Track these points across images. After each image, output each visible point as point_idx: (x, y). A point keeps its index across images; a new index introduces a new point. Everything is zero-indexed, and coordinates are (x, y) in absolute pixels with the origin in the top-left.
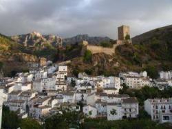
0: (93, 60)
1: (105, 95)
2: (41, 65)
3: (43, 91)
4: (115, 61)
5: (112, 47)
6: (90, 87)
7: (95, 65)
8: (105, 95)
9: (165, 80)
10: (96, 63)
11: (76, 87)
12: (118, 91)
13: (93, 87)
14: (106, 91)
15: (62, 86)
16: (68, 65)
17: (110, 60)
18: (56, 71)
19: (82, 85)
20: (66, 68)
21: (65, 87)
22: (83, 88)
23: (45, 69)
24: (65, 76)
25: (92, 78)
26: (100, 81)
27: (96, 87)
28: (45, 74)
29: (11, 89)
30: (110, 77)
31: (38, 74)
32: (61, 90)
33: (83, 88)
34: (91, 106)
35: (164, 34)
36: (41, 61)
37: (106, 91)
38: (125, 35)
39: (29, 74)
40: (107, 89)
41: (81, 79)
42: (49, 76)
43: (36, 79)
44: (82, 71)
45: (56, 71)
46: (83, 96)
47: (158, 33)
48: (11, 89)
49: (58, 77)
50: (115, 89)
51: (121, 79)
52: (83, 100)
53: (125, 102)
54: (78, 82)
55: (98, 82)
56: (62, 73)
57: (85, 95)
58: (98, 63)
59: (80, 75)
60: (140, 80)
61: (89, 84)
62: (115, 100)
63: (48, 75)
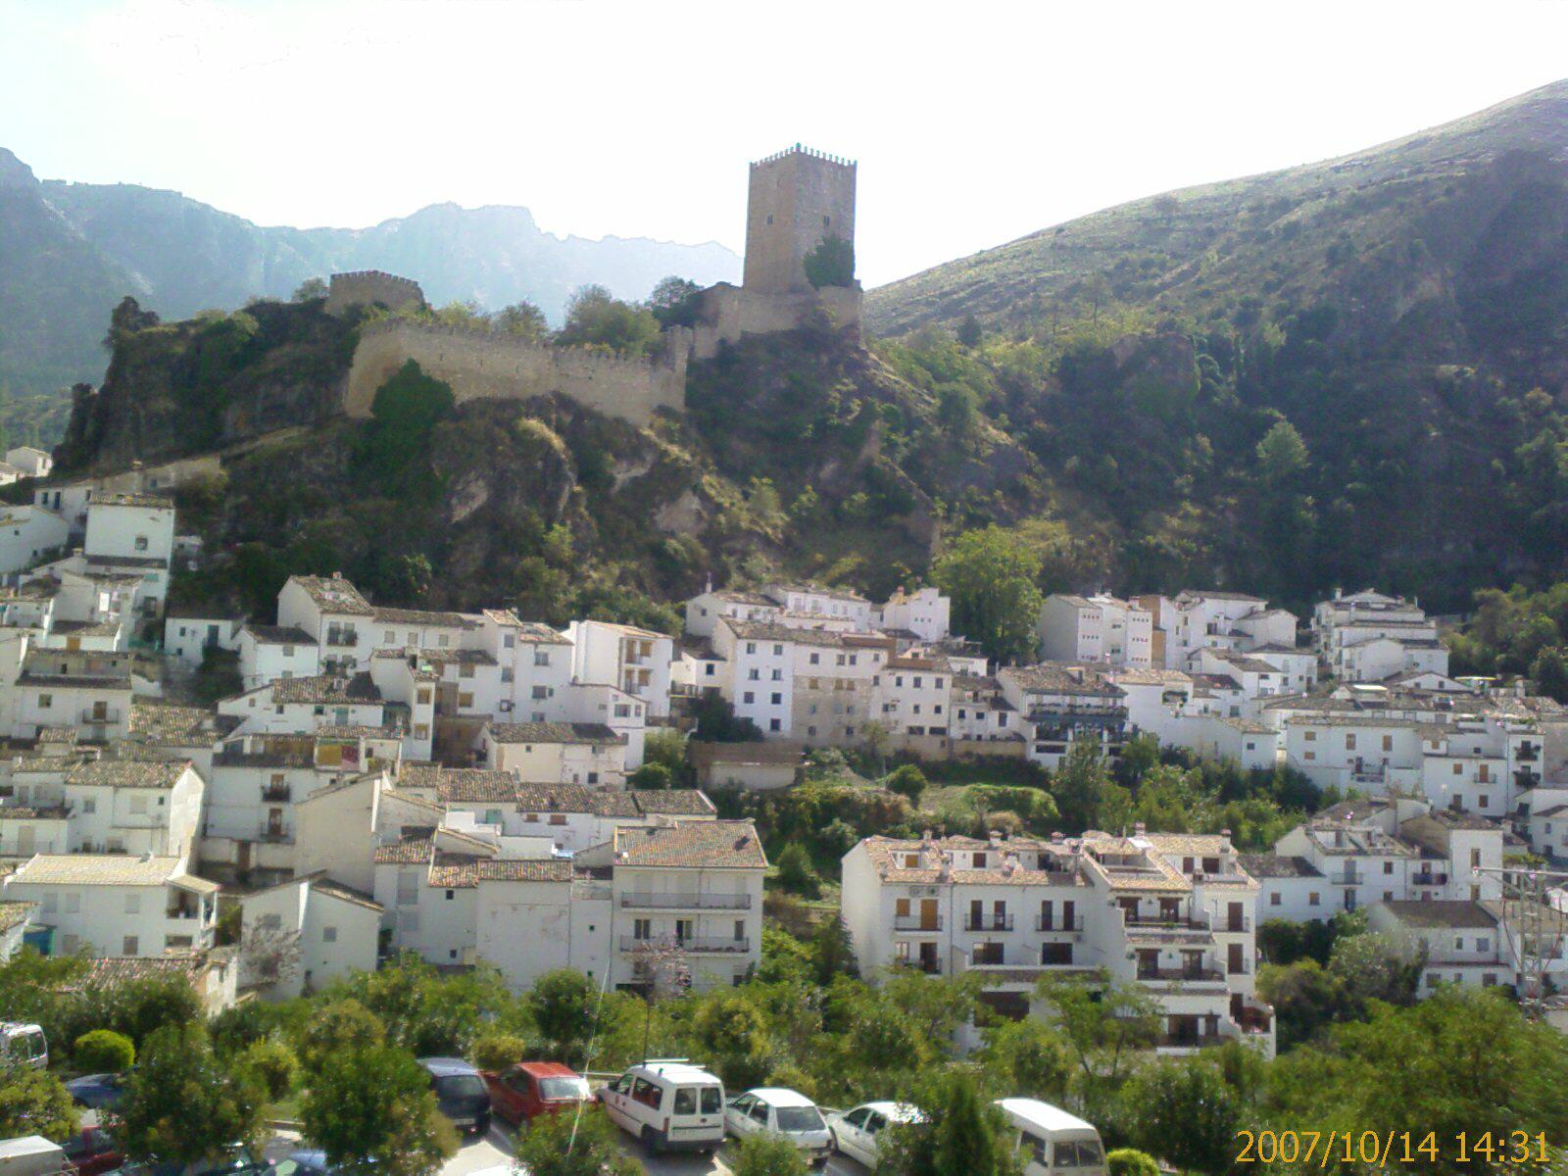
6: (369, 715)
7: (461, 513)
10: (480, 494)
11: (227, 707)
16: (190, 505)
17: (623, 474)
18: (52, 555)
19: (288, 690)
24: (145, 607)
25: (403, 635)
26: (472, 658)
33: (299, 719)
34: (323, 881)
40: (537, 732)
41: (299, 636)
44: (320, 567)
45: (52, 555)
46: (277, 794)
52: (275, 834)
54: (265, 660)
56: (107, 569)
57: (299, 780)
58: (498, 494)
59: (296, 598)
60: (867, 664)
61: (364, 689)
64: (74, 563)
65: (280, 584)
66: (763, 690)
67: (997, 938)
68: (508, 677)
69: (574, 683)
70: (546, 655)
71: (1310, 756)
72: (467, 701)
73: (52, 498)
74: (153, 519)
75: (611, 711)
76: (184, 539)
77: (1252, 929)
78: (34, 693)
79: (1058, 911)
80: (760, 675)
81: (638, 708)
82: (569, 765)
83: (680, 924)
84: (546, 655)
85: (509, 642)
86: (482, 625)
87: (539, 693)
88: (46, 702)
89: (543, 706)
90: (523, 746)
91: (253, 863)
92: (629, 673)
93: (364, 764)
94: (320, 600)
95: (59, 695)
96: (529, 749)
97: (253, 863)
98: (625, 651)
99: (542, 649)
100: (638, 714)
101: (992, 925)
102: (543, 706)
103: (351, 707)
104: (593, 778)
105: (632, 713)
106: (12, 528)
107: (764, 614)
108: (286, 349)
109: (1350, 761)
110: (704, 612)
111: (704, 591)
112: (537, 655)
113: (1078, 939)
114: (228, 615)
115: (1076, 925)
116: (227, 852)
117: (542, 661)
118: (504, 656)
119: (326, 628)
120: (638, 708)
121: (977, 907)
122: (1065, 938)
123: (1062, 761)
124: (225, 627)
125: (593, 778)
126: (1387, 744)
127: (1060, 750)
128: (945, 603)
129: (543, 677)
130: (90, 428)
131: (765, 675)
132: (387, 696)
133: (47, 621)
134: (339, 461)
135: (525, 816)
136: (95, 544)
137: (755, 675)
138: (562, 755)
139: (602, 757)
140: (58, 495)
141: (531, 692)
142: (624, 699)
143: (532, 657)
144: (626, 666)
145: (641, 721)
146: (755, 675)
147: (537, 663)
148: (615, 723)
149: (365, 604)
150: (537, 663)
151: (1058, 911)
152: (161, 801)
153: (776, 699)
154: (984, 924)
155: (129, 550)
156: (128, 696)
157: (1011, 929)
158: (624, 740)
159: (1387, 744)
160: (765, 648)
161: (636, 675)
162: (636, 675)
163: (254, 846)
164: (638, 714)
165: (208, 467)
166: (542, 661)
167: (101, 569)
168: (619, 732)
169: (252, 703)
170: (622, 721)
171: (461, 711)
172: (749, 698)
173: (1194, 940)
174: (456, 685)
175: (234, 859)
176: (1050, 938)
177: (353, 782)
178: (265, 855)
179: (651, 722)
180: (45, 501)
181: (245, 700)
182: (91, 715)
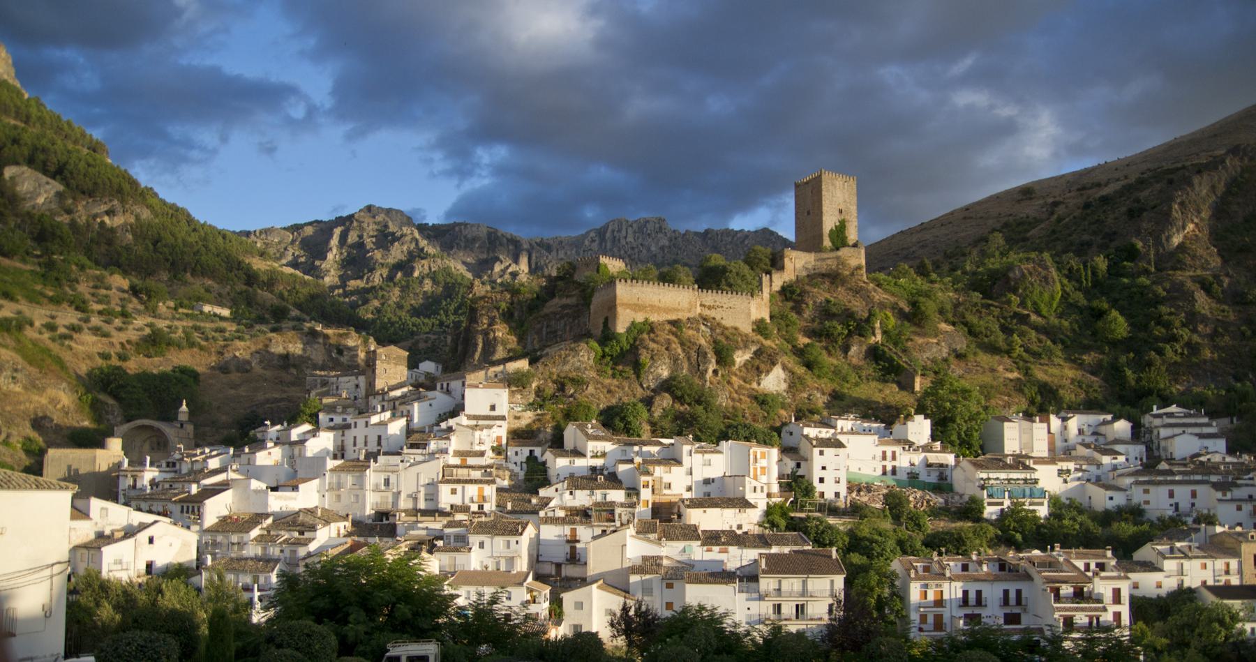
0: (644, 357)
1: (691, 533)
2: (380, 384)
3: (382, 515)
4: (763, 361)
5: (753, 290)
6: (617, 496)
8: (691, 533)
9: (1020, 462)
11: (543, 492)
13: (633, 491)
14: (696, 517)
15: (472, 490)
20: (502, 398)
21: (490, 491)
22: (582, 498)
23: (397, 407)
27: (646, 494)
28: (396, 427)
29: (215, 509)
30: (725, 445)
31: (359, 432)
32: (465, 509)
33: (582, 498)
35: (1061, 210)
36: (380, 366)
37: (696, 517)
38: (829, 222)
39: (314, 433)
42: (415, 439)
43: (350, 454)
47: (1030, 210)
48: (215, 509)
49: (455, 443)
50: (744, 504)
51: (787, 451)
53: (778, 566)
55: (659, 471)
57: (584, 533)
62: (736, 558)
63: (409, 431)
64: (462, 419)
67: (977, 611)
71: (1147, 502)
72: (669, 486)
73: (445, 386)
79: (1012, 595)
81: (762, 488)
86: (673, 444)
88: (454, 492)
90: (702, 510)
91: (563, 574)
93: (618, 524)
94: (587, 434)
97: (563, 574)
99: (707, 456)
100: (762, 491)
103: (608, 491)
105: (759, 489)
106: (428, 402)
107: (825, 433)
108: (556, 301)
109: (1171, 505)
110: (791, 434)
113: (1025, 610)
114: (539, 444)
115: (1023, 603)
116: (549, 569)
120: (762, 488)
124: (538, 451)
125: (740, 527)
126: (1194, 494)
127: (1002, 504)
128: (928, 422)
130: (460, 348)
134: (589, 359)
135: (705, 548)
136: (470, 408)
142: (754, 483)
145: (764, 495)
148: (750, 497)
149: (609, 435)
151: (1012, 595)
152: (517, 542)
154: (970, 603)
155: (487, 412)
156: (494, 487)
157: (986, 606)
159: (1194, 494)
160: (829, 451)
161: (759, 470)
162: (759, 470)
163: (563, 566)
164: (762, 491)
165: (523, 365)
167: (473, 422)
169: (557, 490)
170: (754, 495)
171: (666, 492)
172: (822, 480)
173: (1096, 609)
174: (661, 478)
175: (554, 573)
176: (1008, 611)
177: (614, 531)
178: (568, 571)
179: (769, 495)
180: (442, 388)
181: (553, 488)
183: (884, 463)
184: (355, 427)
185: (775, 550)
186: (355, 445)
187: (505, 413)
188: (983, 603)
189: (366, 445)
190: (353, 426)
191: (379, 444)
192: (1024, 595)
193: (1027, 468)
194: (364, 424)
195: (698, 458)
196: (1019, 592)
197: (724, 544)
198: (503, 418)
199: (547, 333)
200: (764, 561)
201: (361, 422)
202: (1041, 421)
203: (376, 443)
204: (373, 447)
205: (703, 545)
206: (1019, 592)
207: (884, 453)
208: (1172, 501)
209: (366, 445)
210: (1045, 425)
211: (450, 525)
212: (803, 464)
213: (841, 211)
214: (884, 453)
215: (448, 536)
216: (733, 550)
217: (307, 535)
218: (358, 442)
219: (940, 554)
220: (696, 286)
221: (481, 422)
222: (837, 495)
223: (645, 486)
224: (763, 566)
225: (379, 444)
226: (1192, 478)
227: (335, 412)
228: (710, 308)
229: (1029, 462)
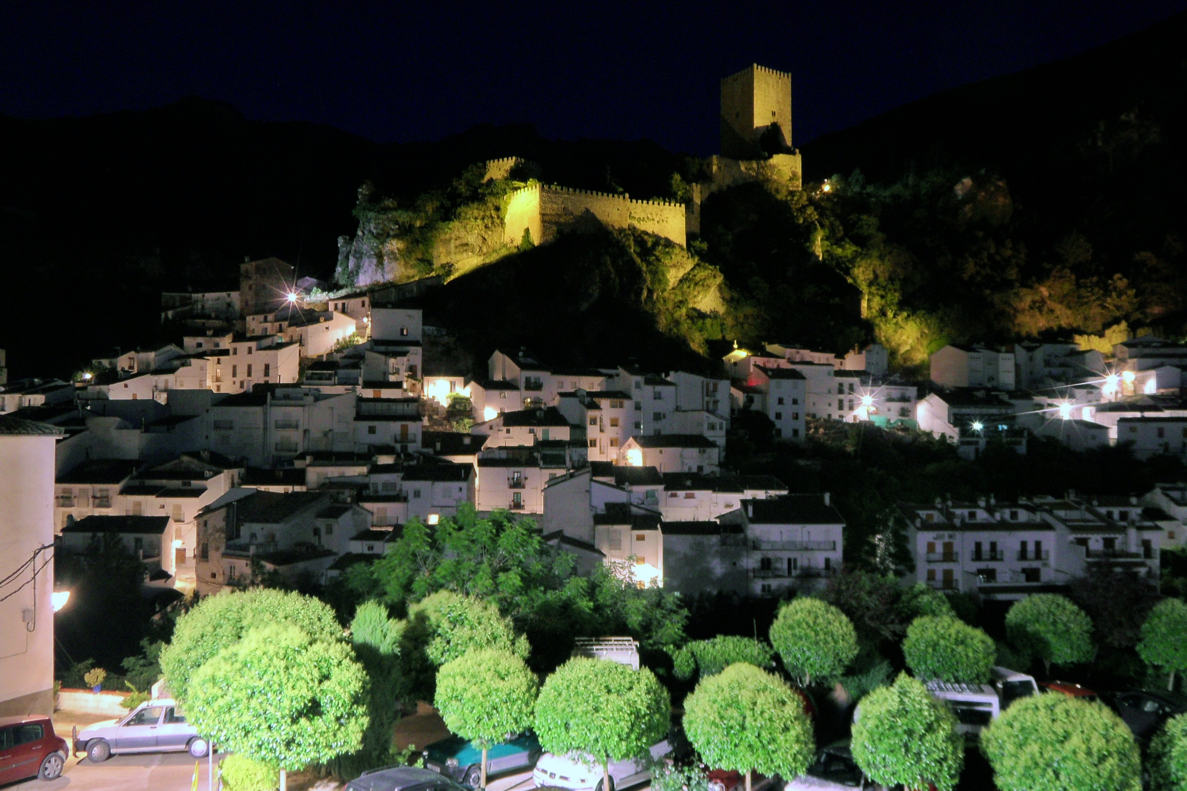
6: (562, 433)
7: (585, 306)
12: (714, 455)
65: (493, 352)
66: (787, 410)
67: (992, 565)
68: (638, 407)
69: (678, 409)
70: (659, 393)
73: (340, 306)
74: (410, 316)
75: (706, 426)
76: (426, 328)
77: (1158, 555)
78: (365, 425)
80: (785, 402)
81: (721, 424)
82: (686, 461)
83: (789, 560)
84: (659, 393)
85: (638, 386)
87: (658, 417)
88: (372, 430)
89: (659, 425)
90: (658, 450)
92: (708, 403)
95: (378, 425)
96: (661, 452)
98: (705, 389)
99: (658, 388)
100: (721, 428)
101: (988, 557)
102: (659, 425)
104: (700, 468)
109: (1161, 445)
111: (733, 349)
112: (655, 393)
113: (1045, 565)
115: (1043, 556)
117: (658, 396)
118: (635, 393)
119: (524, 380)
120: (721, 424)
121: (978, 545)
122: (1035, 564)
123: (977, 450)
129: (660, 406)
131: (788, 401)
132: (570, 420)
133: (361, 381)
135: (670, 493)
137: (781, 401)
138: (681, 456)
139: (705, 455)
140: (344, 304)
141: (652, 416)
143: (651, 394)
144: (706, 399)
146: (781, 401)
147: (655, 398)
148: (709, 435)
150: (655, 398)
153: (796, 417)
155: (397, 337)
157: (1001, 560)
158: (713, 445)
160: (787, 383)
166: (658, 396)
167: (382, 348)
168: (711, 439)
172: (778, 416)
176: (1026, 564)
182: (399, 438)
183: (841, 396)
184: (235, 353)
185: (749, 494)
186: (234, 375)
187: (420, 338)
188: (999, 556)
189: (249, 374)
190: (231, 352)
191: (267, 374)
192: (1044, 547)
193: (1002, 403)
194: (246, 350)
195: (649, 390)
196: (1038, 544)
197: (689, 488)
198: (416, 343)
199: (456, 247)
200: (750, 509)
201: (242, 347)
202: (1007, 352)
203: (263, 373)
204: (258, 378)
205: (666, 489)
206: (1038, 544)
207: (841, 385)
208: (1161, 441)
209: (249, 374)
210: (1011, 356)
211: (376, 469)
212: (757, 397)
213: (774, 114)
214: (841, 385)
215: (375, 485)
216: (703, 495)
217: (196, 483)
218: (238, 371)
219: (944, 500)
220: (627, 195)
221: (391, 348)
222: (796, 432)
223: (594, 421)
224: (750, 514)
225: (267, 374)
226: (1138, 415)
227: (203, 334)
228: (639, 220)
229: (1005, 397)
